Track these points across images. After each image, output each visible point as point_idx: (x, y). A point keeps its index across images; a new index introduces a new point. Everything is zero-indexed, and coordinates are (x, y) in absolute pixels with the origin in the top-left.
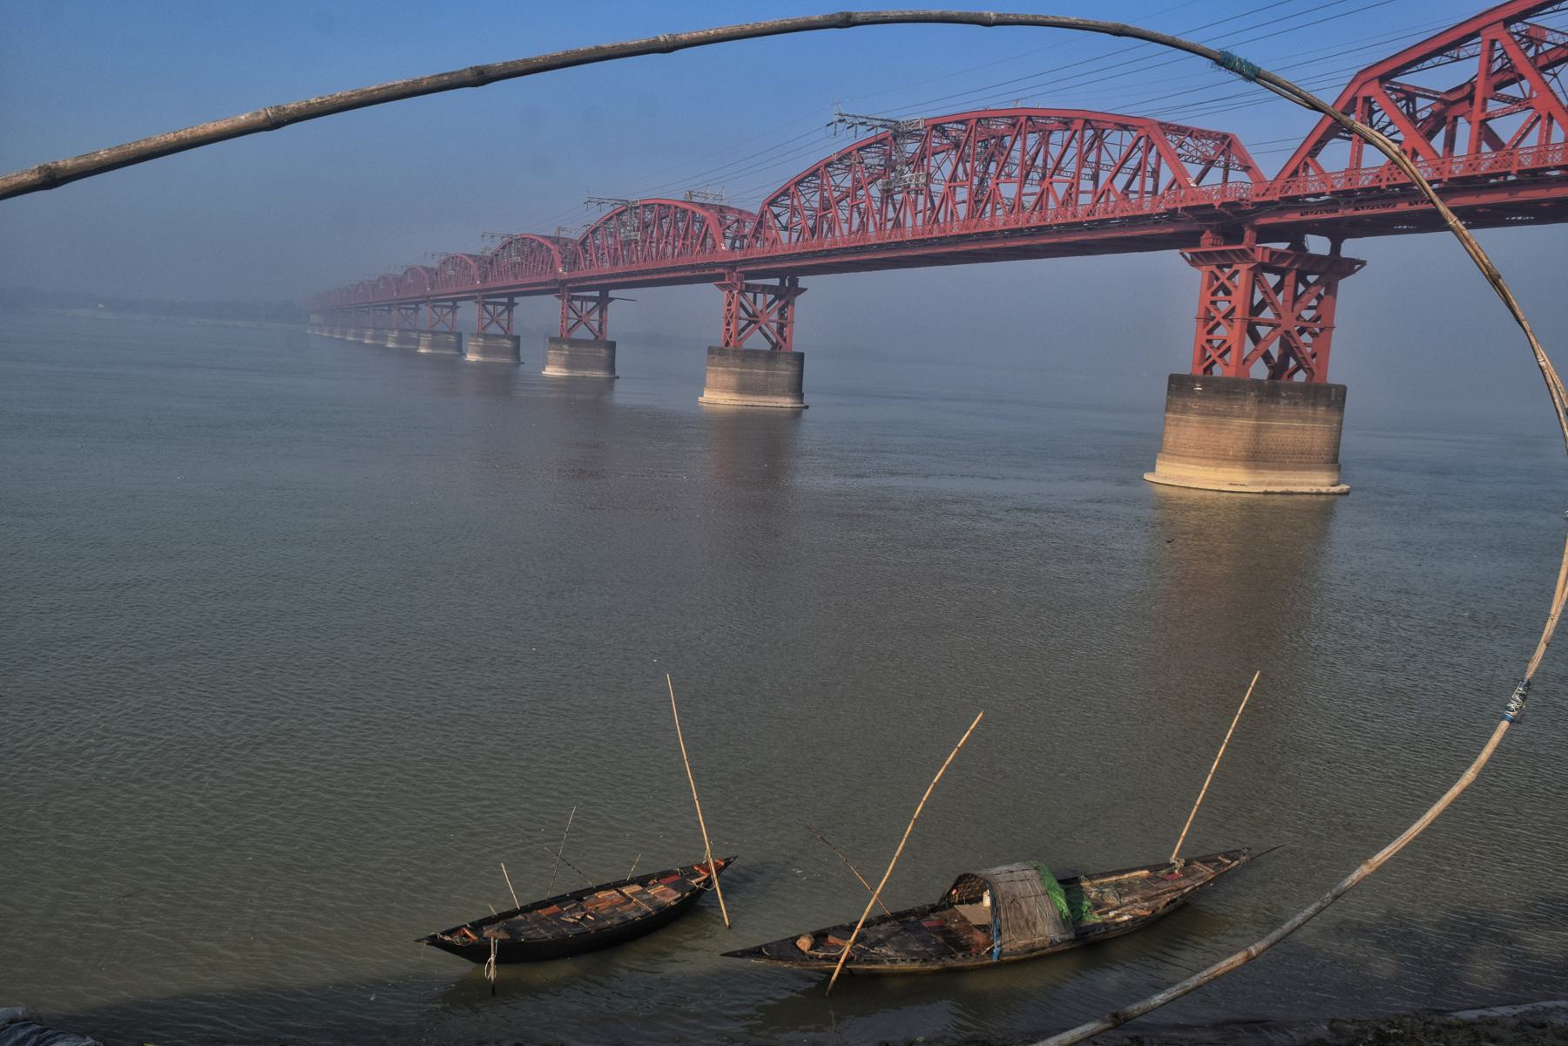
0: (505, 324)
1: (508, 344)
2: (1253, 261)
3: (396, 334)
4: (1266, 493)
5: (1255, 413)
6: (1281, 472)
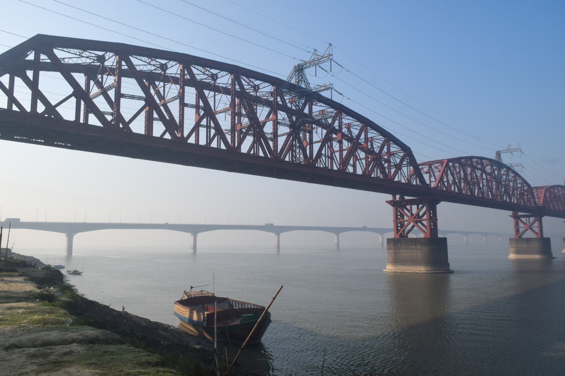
4: (395, 272)
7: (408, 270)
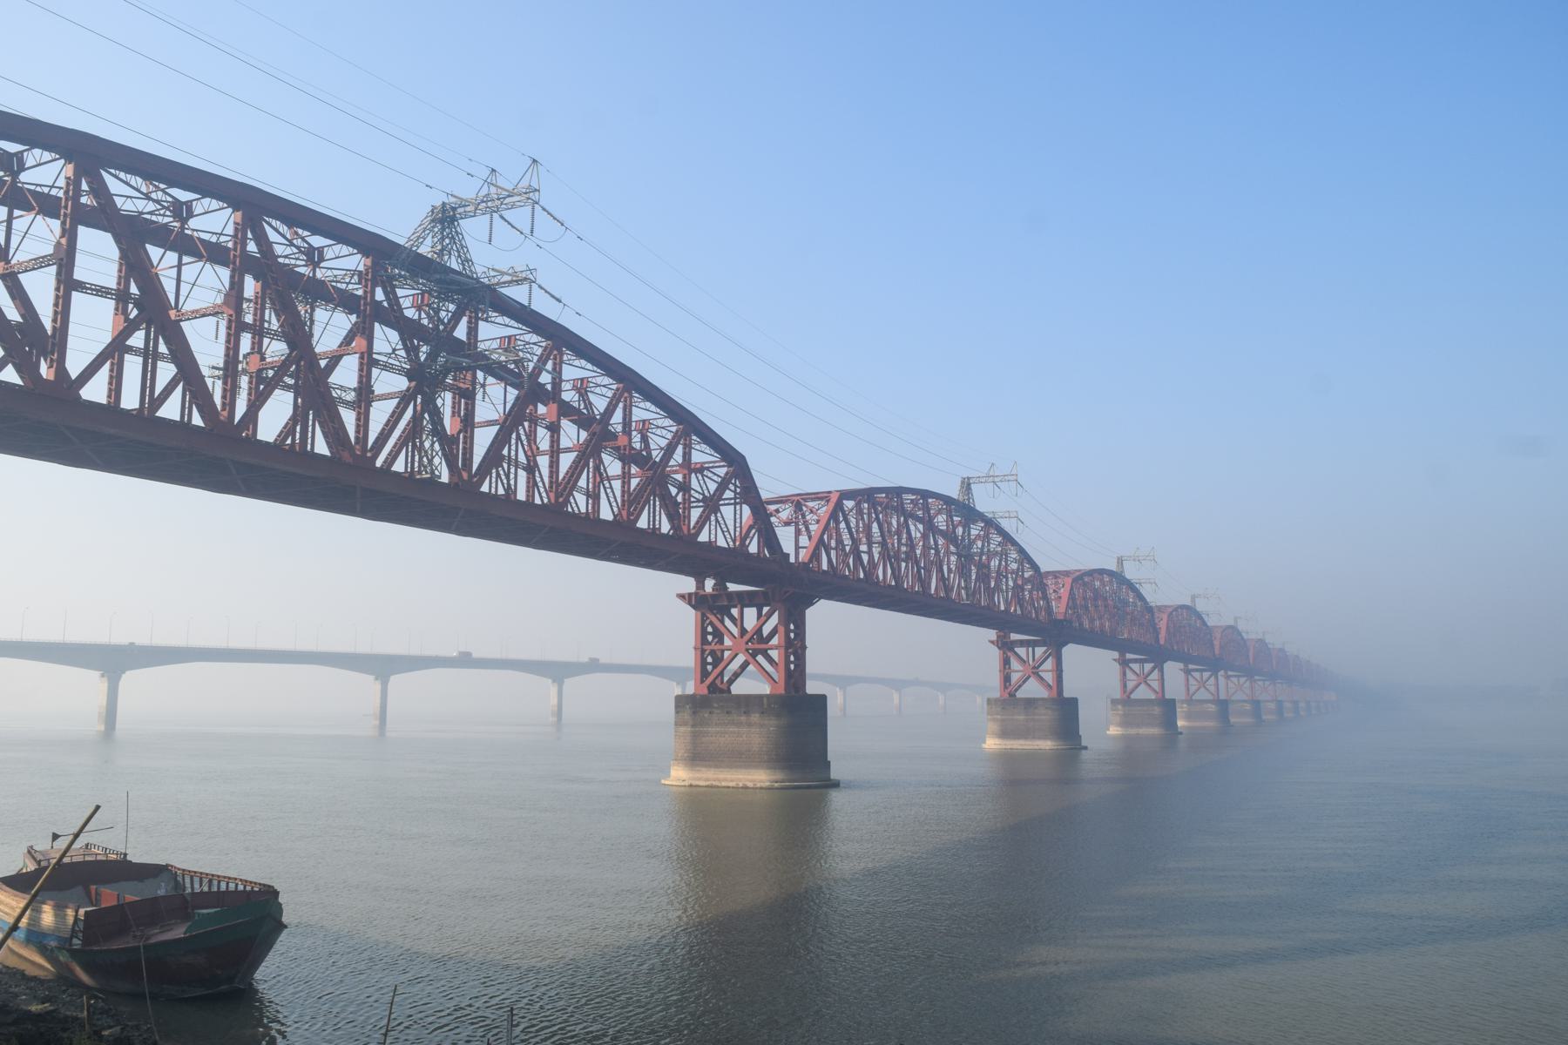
4: (691, 786)
7: (725, 780)
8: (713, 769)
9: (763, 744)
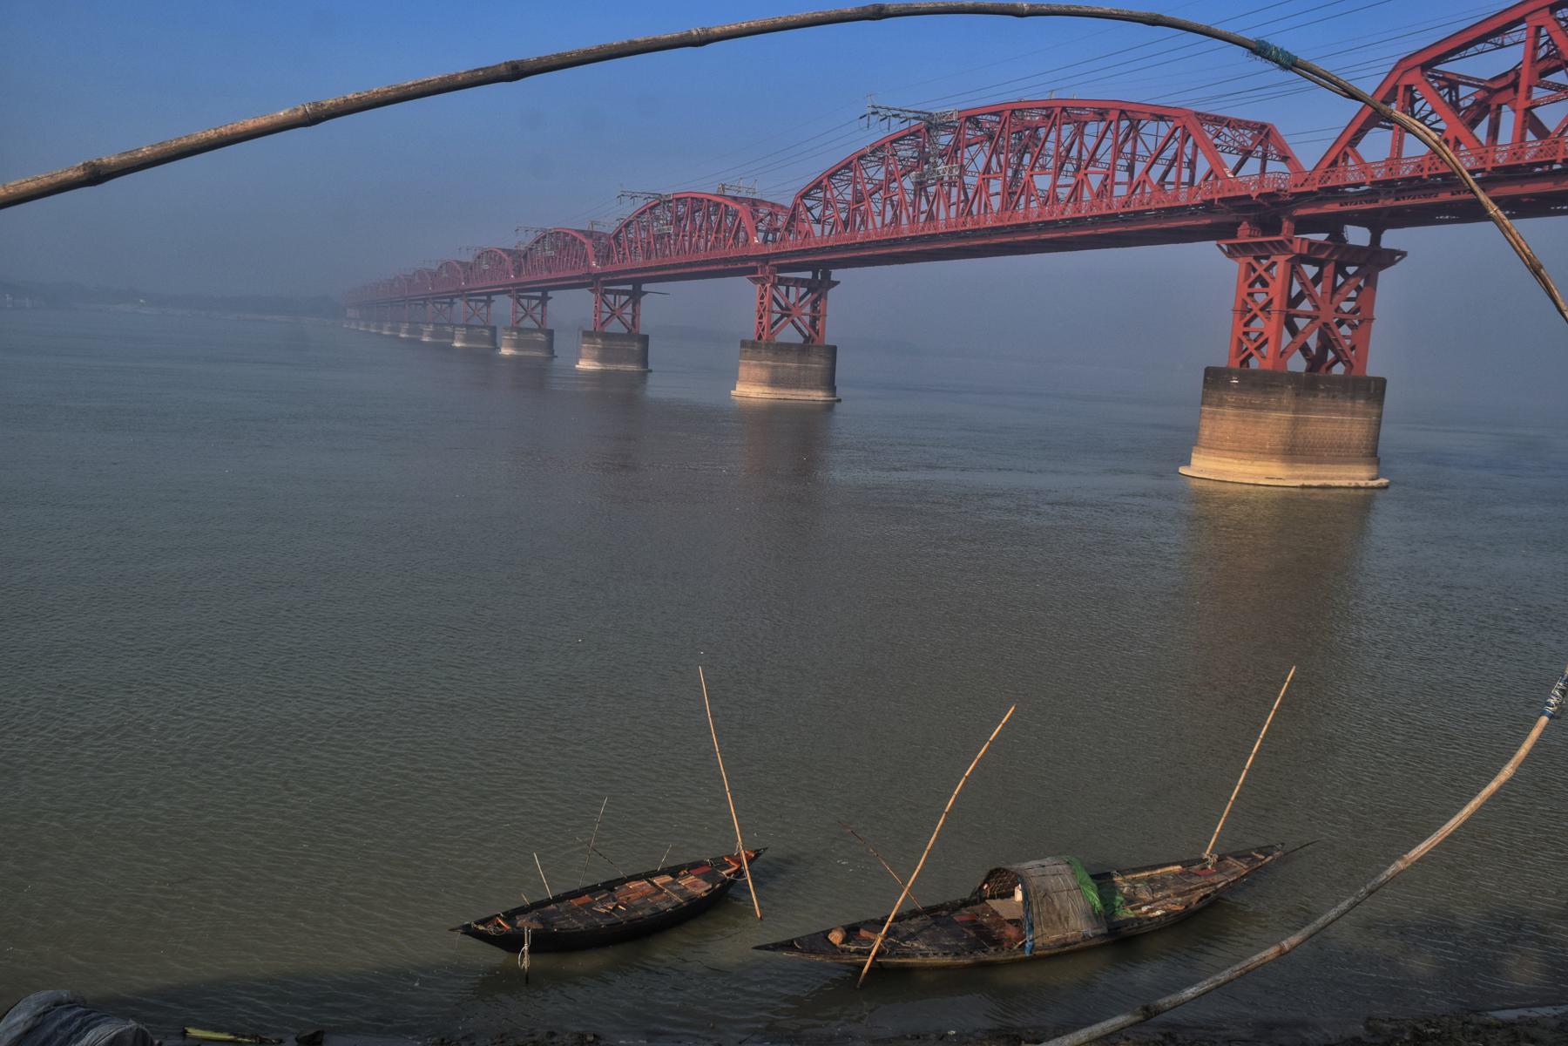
0: (538, 318)
1: (541, 337)
2: (1292, 252)
3: (431, 328)
4: (1303, 487)
5: (1292, 406)
6: (1319, 466)
8: (1314, 465)
9: (1364, 436)
